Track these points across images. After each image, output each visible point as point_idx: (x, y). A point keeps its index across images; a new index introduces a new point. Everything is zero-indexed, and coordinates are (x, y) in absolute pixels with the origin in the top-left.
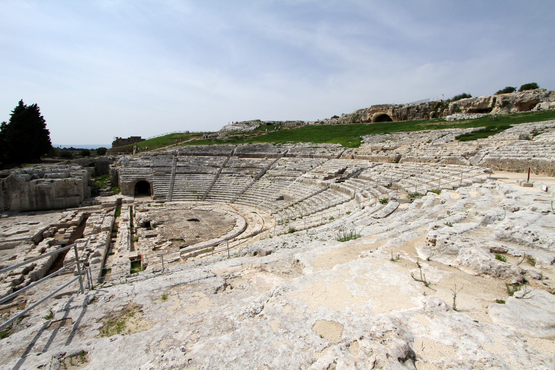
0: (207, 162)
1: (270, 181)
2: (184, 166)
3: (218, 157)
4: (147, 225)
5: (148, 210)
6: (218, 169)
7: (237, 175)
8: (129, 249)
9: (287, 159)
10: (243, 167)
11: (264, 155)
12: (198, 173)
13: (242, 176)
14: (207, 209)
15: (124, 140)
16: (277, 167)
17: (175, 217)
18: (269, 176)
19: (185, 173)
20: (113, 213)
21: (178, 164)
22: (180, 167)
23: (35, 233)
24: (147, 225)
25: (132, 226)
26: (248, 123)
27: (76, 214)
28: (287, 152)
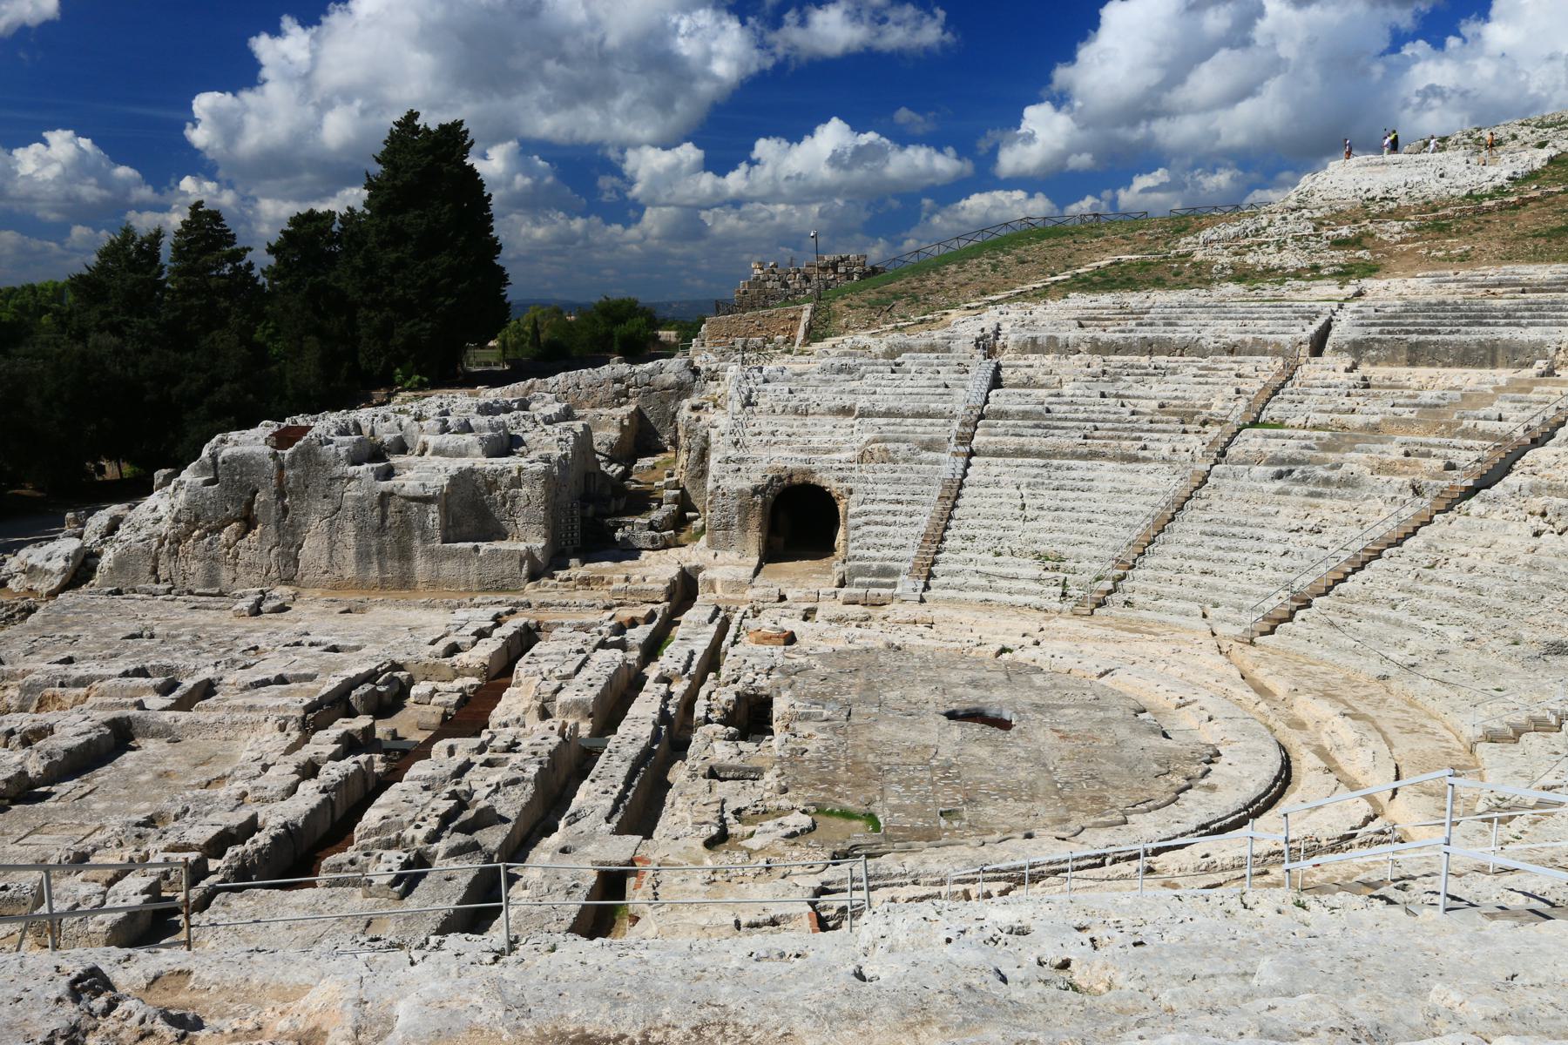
1: (1536, 522)
2: (1025, 415)
5: (790, 639)
6: (1213, 431)
7: (1321, 472)
8: (616, 818)
11: (1539, 348)
12: (1093, 455)
18: (1535, 490)
19: (1022, 453)
23: (324, 691)
27: (498, 625)
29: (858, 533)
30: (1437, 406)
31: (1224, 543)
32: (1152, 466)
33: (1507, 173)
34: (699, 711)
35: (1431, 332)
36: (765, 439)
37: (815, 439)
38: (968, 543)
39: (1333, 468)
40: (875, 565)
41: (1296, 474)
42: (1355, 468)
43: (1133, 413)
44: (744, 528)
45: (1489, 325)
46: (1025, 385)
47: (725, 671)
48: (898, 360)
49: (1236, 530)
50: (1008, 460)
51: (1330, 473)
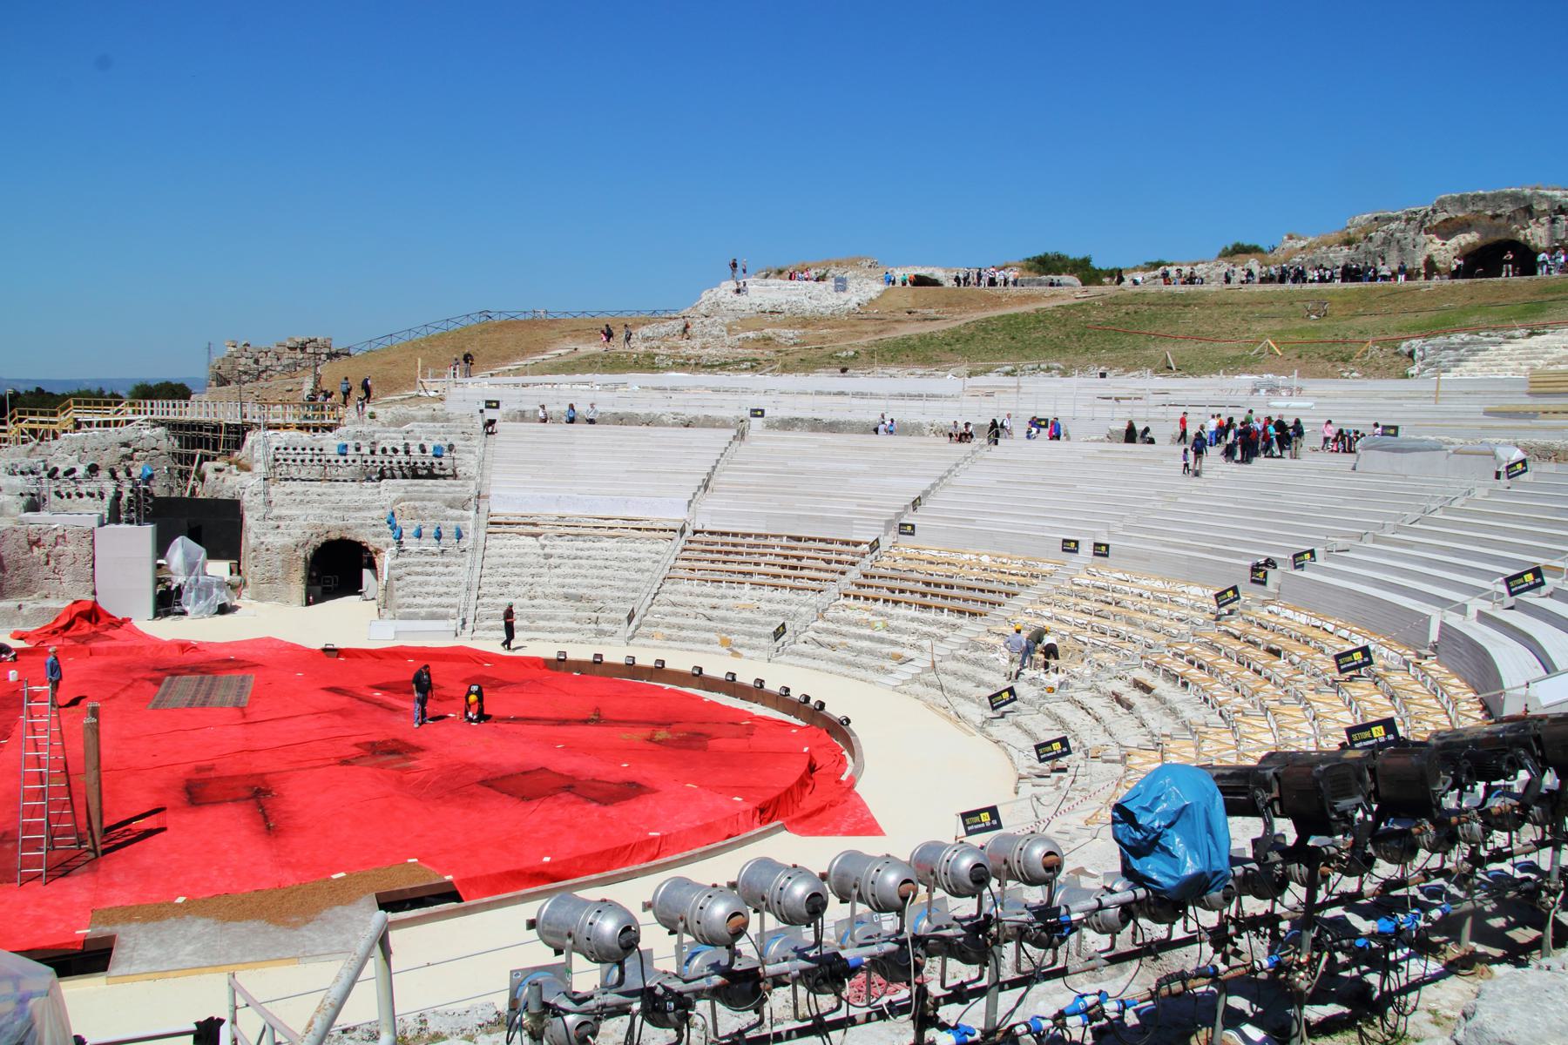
29: (401, 583)
33: (856, 299)
36: (299, 498)
37: (345, 498)
38: (504, 590)
40: (423, 611)
44: (287, 579)
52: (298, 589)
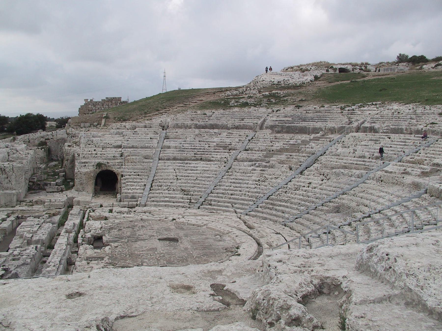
0: (215, 139)
3: (235, 131)
4: (97, 241)
5: (106, 219)
7: (264, 164)
9: (360, 135)
10: (277, 151)
13: (272, 167)
14: (200, 223)
15: (95, 104)
16: (340, 150)
17: (141, 232)
19: (175, 159)
20: (57, 219)
21: (166, 143)
22: (169, 147)
24: (97, 241)
25: (75, 241)
26: (302, 70)
27: (9, 217)
28: (363, 123)
30: (295, 144)
31: (238, 185)
32: (216, 162)
34: (80, 241)
35: (292, 123)
38: (160, 188)
39: (267, 163)
41: (257, 165)
42: (273, 163)
43: (209, 147)
45: (307, 121)
46: (175, 138)
47: (86, 228)
48: (135, 130)
49: (240, 181)
50: (171, 161)
51: (266, 164)
52: (91, 188)
